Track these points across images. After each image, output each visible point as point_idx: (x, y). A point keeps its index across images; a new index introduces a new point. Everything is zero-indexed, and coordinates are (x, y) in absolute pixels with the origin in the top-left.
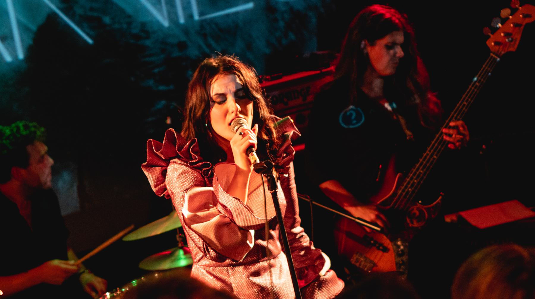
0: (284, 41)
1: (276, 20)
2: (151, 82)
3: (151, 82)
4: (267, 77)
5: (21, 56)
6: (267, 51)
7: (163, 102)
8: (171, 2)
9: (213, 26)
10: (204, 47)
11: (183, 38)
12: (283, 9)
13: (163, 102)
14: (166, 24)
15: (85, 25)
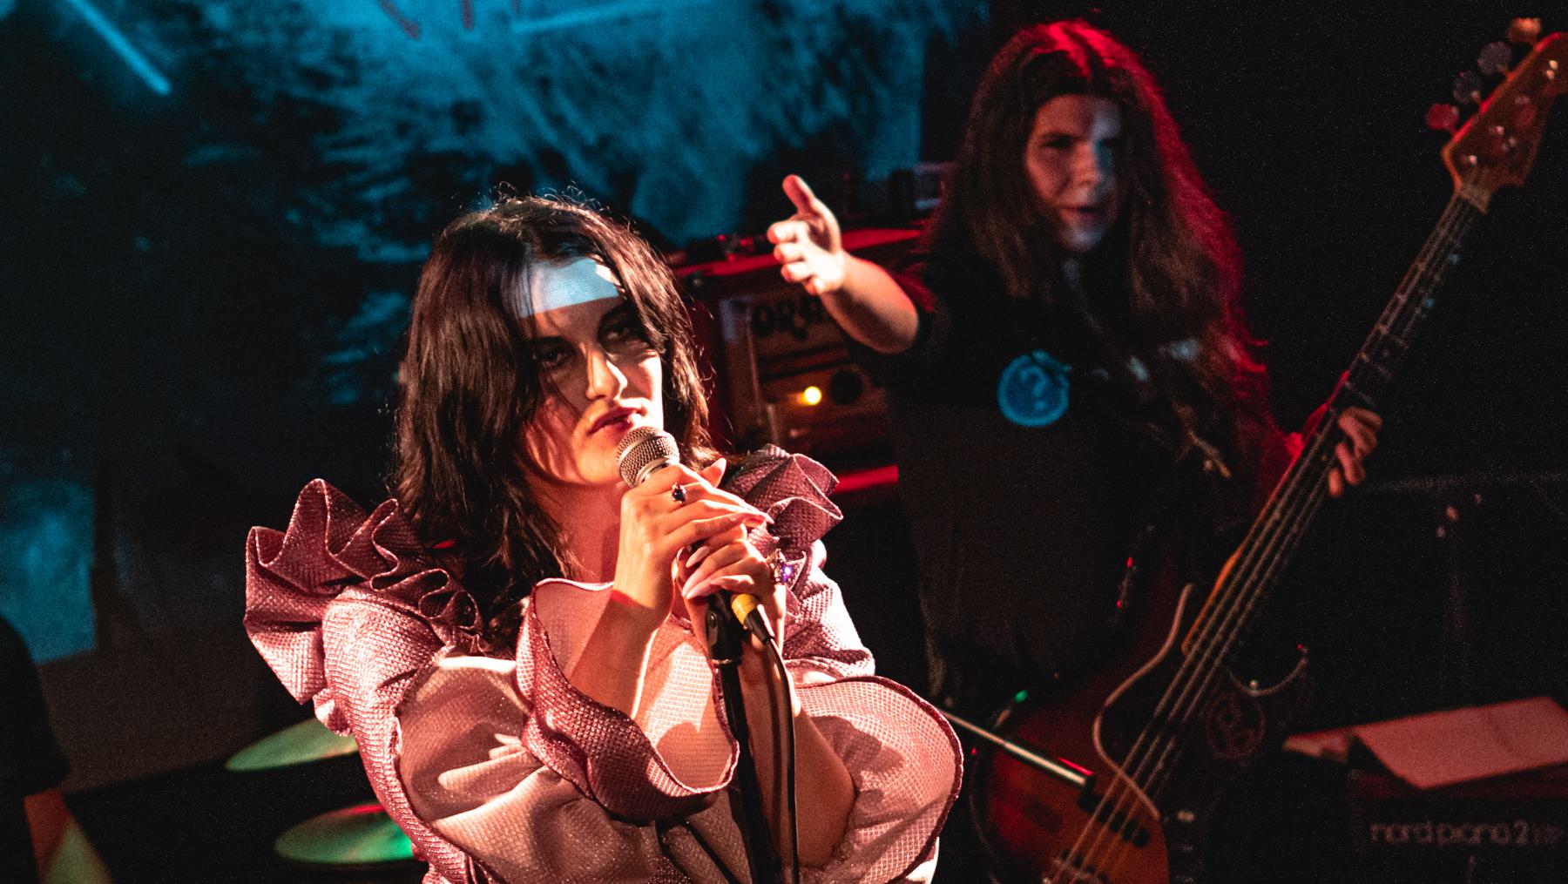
1: (786, 45)
2: (353, 233)
3: (353, 233)
4: (743, 242)
6: (752, 147)
9: (575, 54)
10: (540, 120)
11: (471, 90)
15: (144, 27)
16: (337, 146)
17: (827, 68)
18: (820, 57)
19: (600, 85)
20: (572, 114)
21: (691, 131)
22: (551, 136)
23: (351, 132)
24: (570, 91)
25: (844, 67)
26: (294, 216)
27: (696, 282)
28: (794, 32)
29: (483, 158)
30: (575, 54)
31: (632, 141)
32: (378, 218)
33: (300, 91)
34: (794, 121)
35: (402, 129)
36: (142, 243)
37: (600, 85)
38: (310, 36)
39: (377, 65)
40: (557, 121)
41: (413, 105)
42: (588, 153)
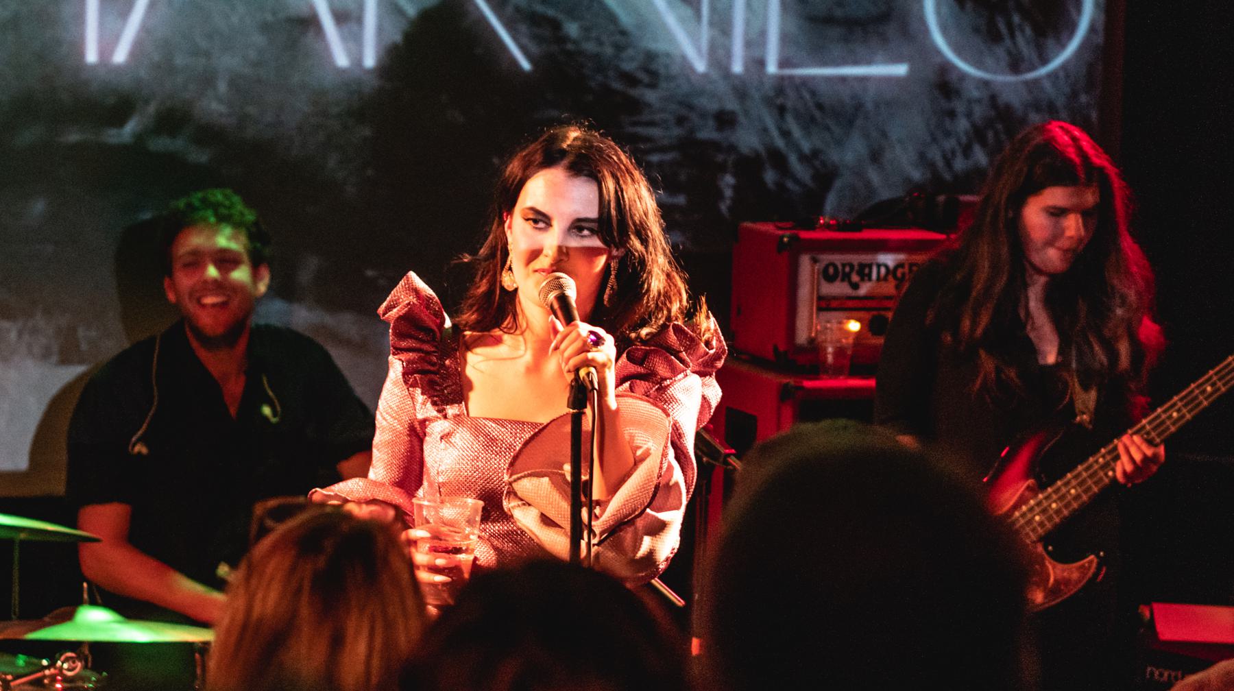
0: (959, 164)
1: (952, 114)
5: (370, 61)
6: (917, 175)
8: (722, 24)
9: (807, 96)
10: (775, 133)
11: (732, 105)
12: (975, 94)
14: (700, 66)
15: (523, 28)
16: (635, 124)
17: (978, 133)
18: (974, 125)
19: (817, 114)
20: (797, 132)
21: (875, 156)
22: (780, 143)
23: (645, 117)
24: (798, 116)
25: (990, 135)
27: (785, 239)
28: (960, 107)
29: (732, 148)
31: (834, 156)
33: (617, 85)
34: (948, 163)
35: (681, 121)
37: (817, 114)
38: (630, 52)
39: (670, 78)
40: (786, 134)
41: (691, 107)
42: (803, 158)
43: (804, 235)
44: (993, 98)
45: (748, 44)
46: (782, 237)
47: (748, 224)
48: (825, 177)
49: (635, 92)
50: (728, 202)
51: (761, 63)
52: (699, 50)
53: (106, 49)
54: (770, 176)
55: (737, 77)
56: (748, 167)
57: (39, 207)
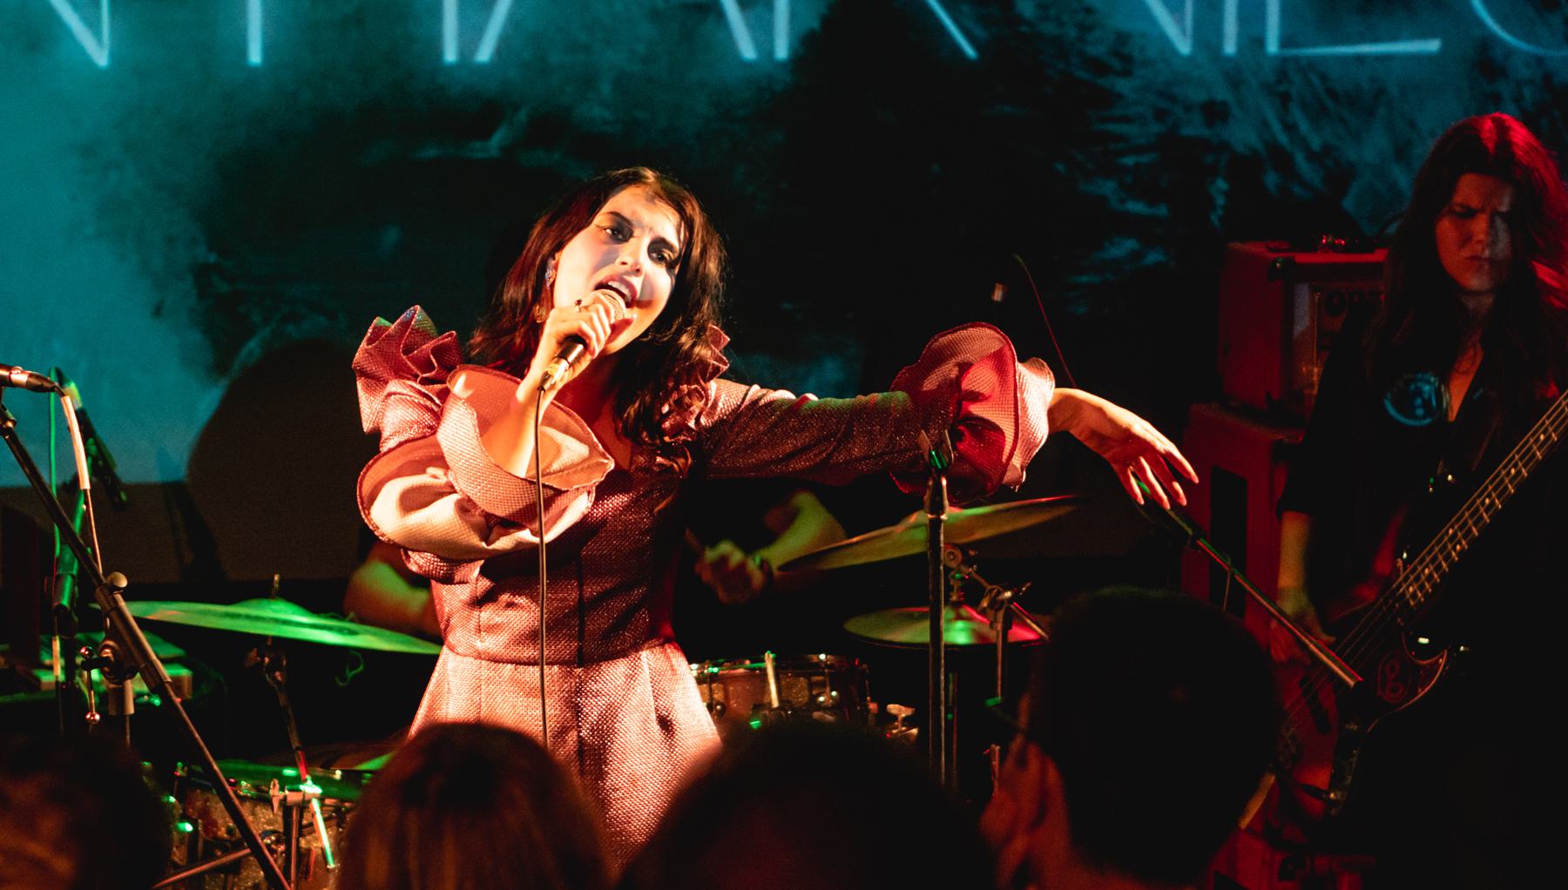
2: (1108, 187)
3: (1108, 187)
5: (782, 51)
7: (1130, 244)
9: (1316, 81)
10: (1276, 127)
11: (1222, 94)
12: (1525, 73)
13: (1130, 244)
14: (1184, 47)
15: (965, 8)
19: (1330, 104)
20: (1304, 126)
22: (1283, 138)
26: (1060, 167)
27: (1278, 265)
28: (1505, 88)
29: (1224, 146)
30: (1316, 81)
31: (1350, 153)
32: (1128, 180)
33: (1081, 74)
35: (1160, 115)
36: (936, 168)
37: (1330, 104)
40: (1290, 128)
41: (1173, 99)
42: (1311, 156)
43: (1302, 258)
44: (1548, 78)
45: (1243, 19)
46: (1275, 261)
47: (1237, 245)
48: (1340, 175)
49: (1102, 81)
50: (1220, 212)
51: (1260, 42)
52: (1184, 32)
53: (469, 42)
54: (1271, 179)
55: (1229, 59)
56: (1244, 168)
57: (392, 236)
